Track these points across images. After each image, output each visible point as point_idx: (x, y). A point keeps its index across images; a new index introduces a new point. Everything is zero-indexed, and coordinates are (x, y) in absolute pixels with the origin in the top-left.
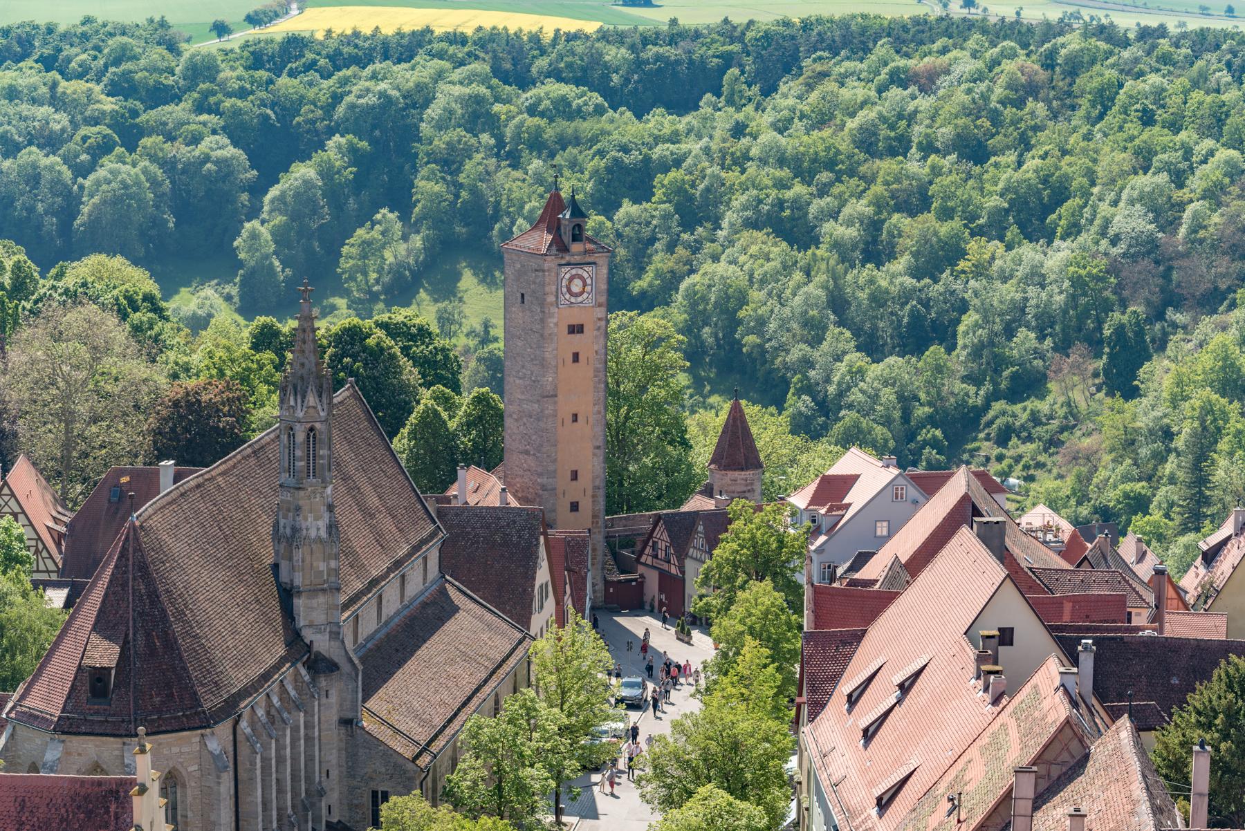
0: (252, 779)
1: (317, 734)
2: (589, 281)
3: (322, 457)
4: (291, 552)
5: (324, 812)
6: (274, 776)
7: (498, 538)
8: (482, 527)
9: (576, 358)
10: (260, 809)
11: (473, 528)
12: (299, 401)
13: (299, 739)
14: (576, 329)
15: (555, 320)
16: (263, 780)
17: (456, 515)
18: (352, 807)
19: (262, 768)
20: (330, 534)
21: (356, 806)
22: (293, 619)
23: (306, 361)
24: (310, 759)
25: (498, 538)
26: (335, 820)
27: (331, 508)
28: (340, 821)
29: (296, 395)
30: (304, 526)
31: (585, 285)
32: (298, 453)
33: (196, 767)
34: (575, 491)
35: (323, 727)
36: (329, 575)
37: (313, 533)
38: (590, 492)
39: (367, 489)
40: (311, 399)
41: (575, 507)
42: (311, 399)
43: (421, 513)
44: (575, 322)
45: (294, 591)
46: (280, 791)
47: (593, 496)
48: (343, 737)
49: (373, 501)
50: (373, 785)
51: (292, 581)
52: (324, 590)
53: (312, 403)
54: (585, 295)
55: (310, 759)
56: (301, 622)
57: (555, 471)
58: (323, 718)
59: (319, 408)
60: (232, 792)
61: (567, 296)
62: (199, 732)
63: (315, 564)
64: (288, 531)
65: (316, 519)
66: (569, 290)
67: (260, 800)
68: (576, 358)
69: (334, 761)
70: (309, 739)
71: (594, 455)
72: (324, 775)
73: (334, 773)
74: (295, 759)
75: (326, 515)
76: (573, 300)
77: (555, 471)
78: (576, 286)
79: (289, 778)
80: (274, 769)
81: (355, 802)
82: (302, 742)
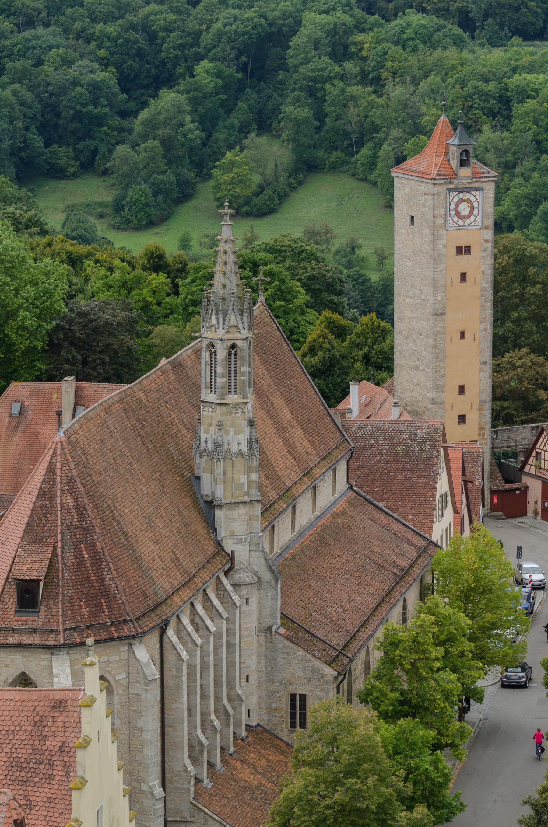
0: (178, 686)
1: (237, 640)
2: (476, 205)
3: (243, 374)
4: (212, 465)
5: (244, 715)
6: (199, 682)
7: (400, 450)
8: (385, 440)
9: (463, 277)
10: (186, 714)
11: (377, 441)
12: (221, 320)
13: (222, 646)
14: (463, 250)
15: (444, 242)
16: (188, 686)
17: (360, 428)
18: (271, 710)
19: (188, 674)
20: (251, 448)
21: (275, 709)
22: (215, 530)
23: (227, 282)
24: (231, 664)
25: (400, 450)
26: (254, 724)
27: (251, 423)
28: (258, 725)
29: (217, 314)
30: (225, 441)
31: (472, 208)
32: (220, 370)
33: (123, 675)
34: (462, 405)
35: (243, 633)
36: (249, 487)
37: (234, 448)
38: (476, 406)
39: (279, 402)
40: (233, 318)
41: (462, 419)
42: (233, 318)
43: (331, 426)
44: (463, 244)
45: (215, 503)
46: (204, 697)
47: (480, 410)
48: (263, 642)
49: (286, 415)
50: (291, 689)
51: (213, 493)
52: (244, 503)
53: (233, 322)
54: (472, 218)
55: (231, 664)
56: (222, 533)
57: (443, 386)
58: (243, 626)
59: (240, 326)
60: (159, 698)
61: (456, 219)
62: (127, 641)
63: (236, 477)
64: (210, 446)
65: (237, 432)
66: (457, 213)
67: (185, 706)
68: (463, 277)
69: (254, 667)
70: (230, 646)
71: (481, 370)
72: (244, 680)
73: (253, 678)
74: (217, 666)
75: (247, 430)
76: (461, 222)
77: (443, 386)
78: (464, 209)
79: (212, 684)
80: (198, 676)
81: (274, 705)
82: (224, 648)
